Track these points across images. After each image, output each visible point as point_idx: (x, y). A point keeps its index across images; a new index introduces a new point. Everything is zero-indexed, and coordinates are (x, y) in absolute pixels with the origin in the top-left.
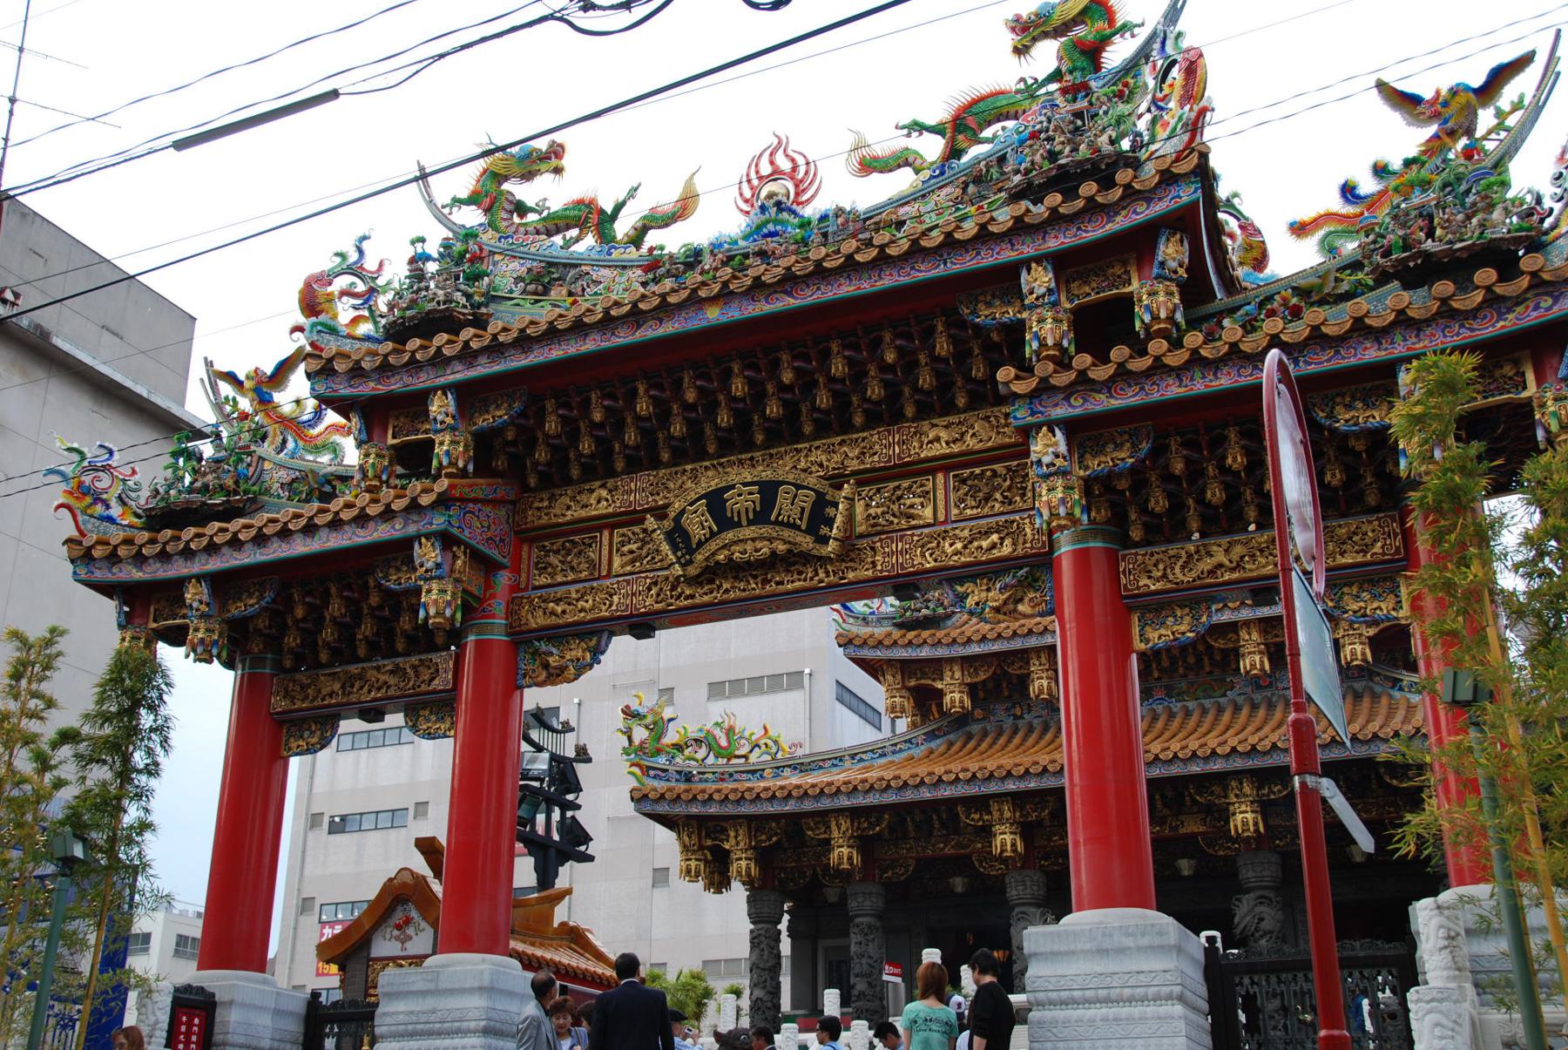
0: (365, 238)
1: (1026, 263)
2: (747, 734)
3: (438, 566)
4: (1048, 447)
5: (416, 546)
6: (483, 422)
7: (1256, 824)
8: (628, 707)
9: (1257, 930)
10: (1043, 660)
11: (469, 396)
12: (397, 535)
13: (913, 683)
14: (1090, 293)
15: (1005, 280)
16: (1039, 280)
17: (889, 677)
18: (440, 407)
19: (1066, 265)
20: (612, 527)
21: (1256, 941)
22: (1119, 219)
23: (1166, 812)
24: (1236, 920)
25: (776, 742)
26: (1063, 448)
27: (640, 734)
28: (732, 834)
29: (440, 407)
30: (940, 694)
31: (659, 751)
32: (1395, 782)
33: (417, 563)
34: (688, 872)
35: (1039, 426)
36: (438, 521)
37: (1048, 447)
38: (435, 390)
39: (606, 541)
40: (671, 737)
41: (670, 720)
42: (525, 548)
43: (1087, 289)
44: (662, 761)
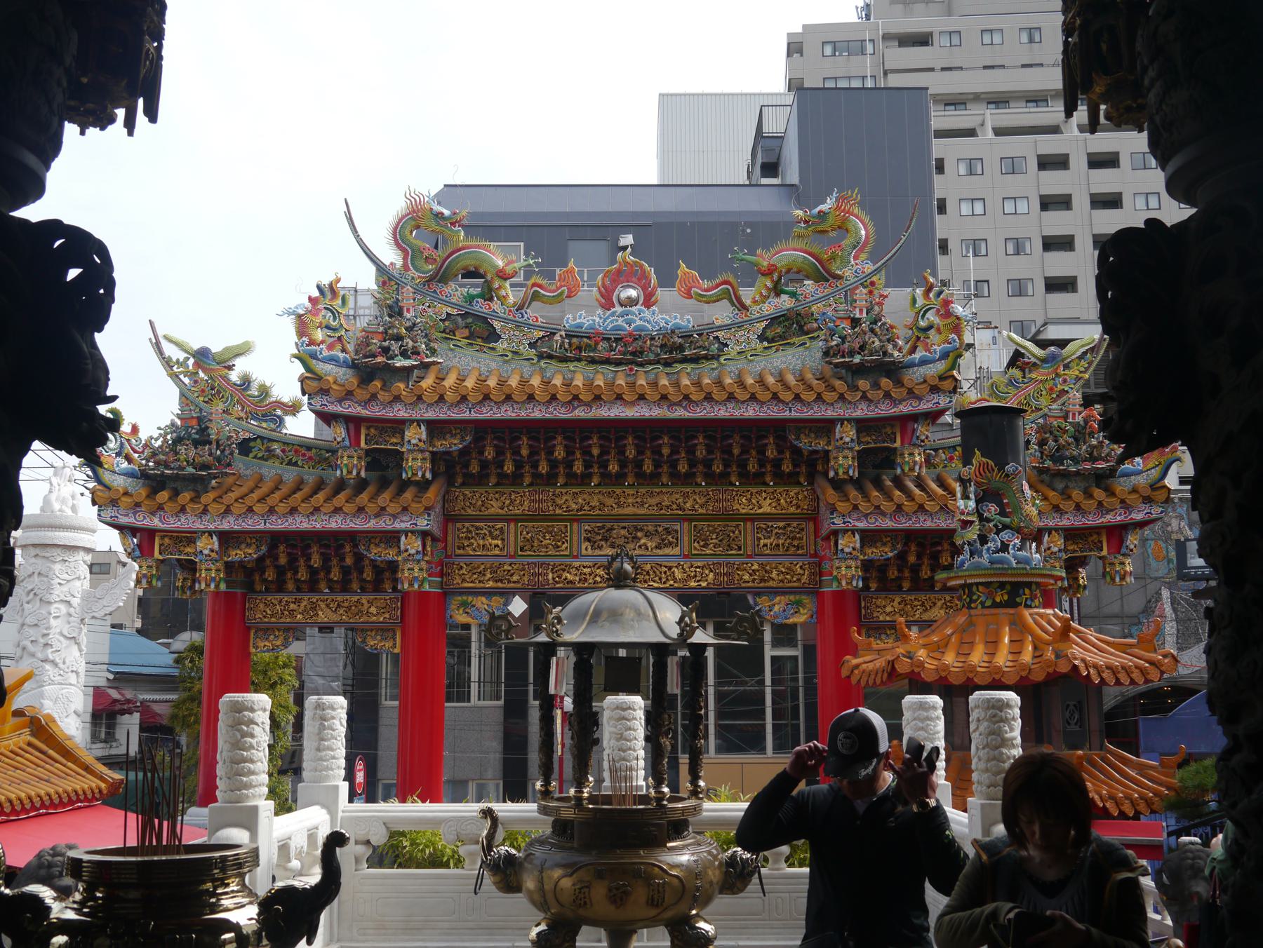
0: (338, 280)
1: (842, 421)
3: (418, 552)
4: (848, 543)
5: (403, 538)
6: (440, 445)
11: (436, 428)
12: (390, 528)
14: (870, 442)
15: (825, 427)
16: (848, 434)
18: (415, 435)
19: (863, 425)
20: (516, 521)
22: (901, 407)
26: (858, 545)
29: (415, 435)
33: (402, 547)
35: (845, 531)
36: (423, 524)
37: (848, 543)
38: (412, 421)
39: (512, 531)
42: (450, 526)
43: (868, 439)
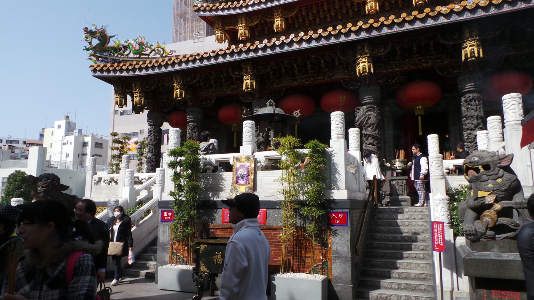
2: (149, 45)
7: (370, 69)
8: (87, 28)
9: (366, 124)
10: (279, 13)
13: (227, 28)
17: (217, 25)
21: (366, 128)
23: (326, 69)
24: (357, 119)
25: (163, 49)
27: (95, 42)
28: (133, 86)
30: (237, 31)
31: (105, 51)
32: (446, 42)
34: (117, 103)
40: (111, 44)
41: (110, 37)
44: (106, 54)
